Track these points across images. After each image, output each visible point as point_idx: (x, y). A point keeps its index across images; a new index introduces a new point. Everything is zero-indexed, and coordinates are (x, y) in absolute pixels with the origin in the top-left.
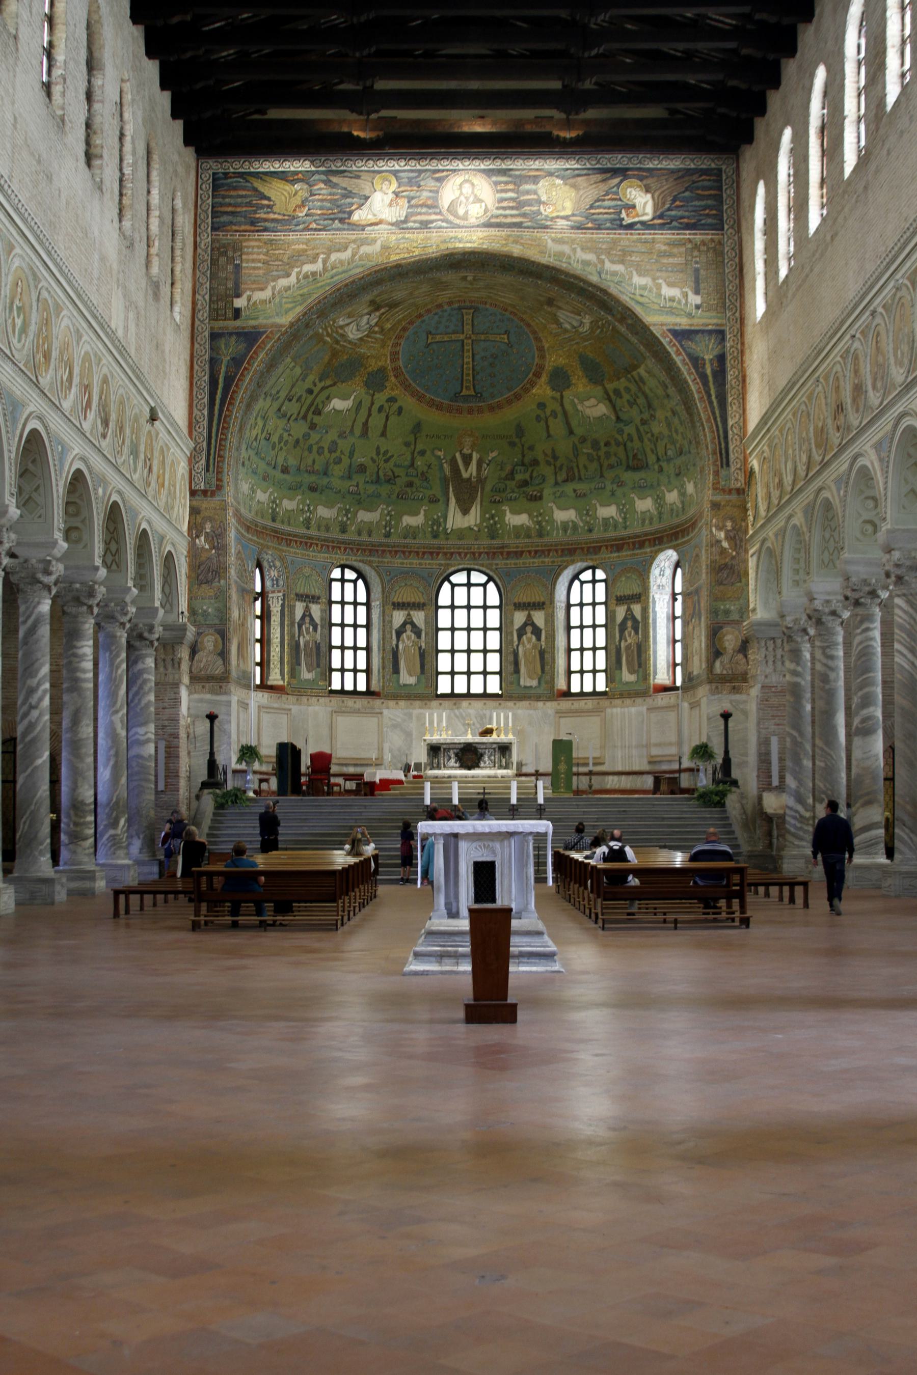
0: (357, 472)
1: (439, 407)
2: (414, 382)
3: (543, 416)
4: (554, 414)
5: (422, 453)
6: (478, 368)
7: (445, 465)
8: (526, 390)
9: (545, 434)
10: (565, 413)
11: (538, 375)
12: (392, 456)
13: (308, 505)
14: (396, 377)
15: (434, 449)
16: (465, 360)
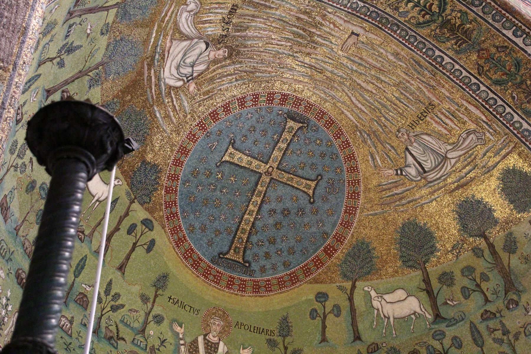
0: (76, 302)
1: (196, 264)
2: (183, 211)
3: (320, 312)
4: (337, 310)
5: (159, 319)
6: (259, 224)
7: (182, 348)
8: (307, 271)
9: (319, 337)
10: (353, 310)
11: (329, 251)
12: (123, 306)
13: (8, 300)
14: (167, 192)
15: (174, 321)
16: (251, 207)
